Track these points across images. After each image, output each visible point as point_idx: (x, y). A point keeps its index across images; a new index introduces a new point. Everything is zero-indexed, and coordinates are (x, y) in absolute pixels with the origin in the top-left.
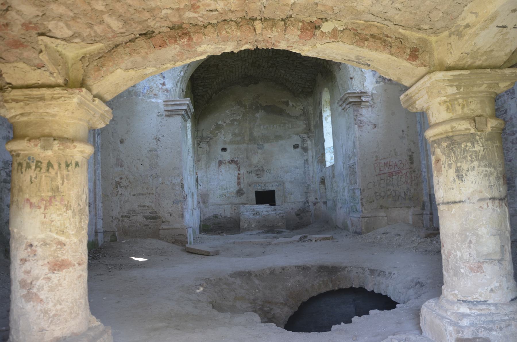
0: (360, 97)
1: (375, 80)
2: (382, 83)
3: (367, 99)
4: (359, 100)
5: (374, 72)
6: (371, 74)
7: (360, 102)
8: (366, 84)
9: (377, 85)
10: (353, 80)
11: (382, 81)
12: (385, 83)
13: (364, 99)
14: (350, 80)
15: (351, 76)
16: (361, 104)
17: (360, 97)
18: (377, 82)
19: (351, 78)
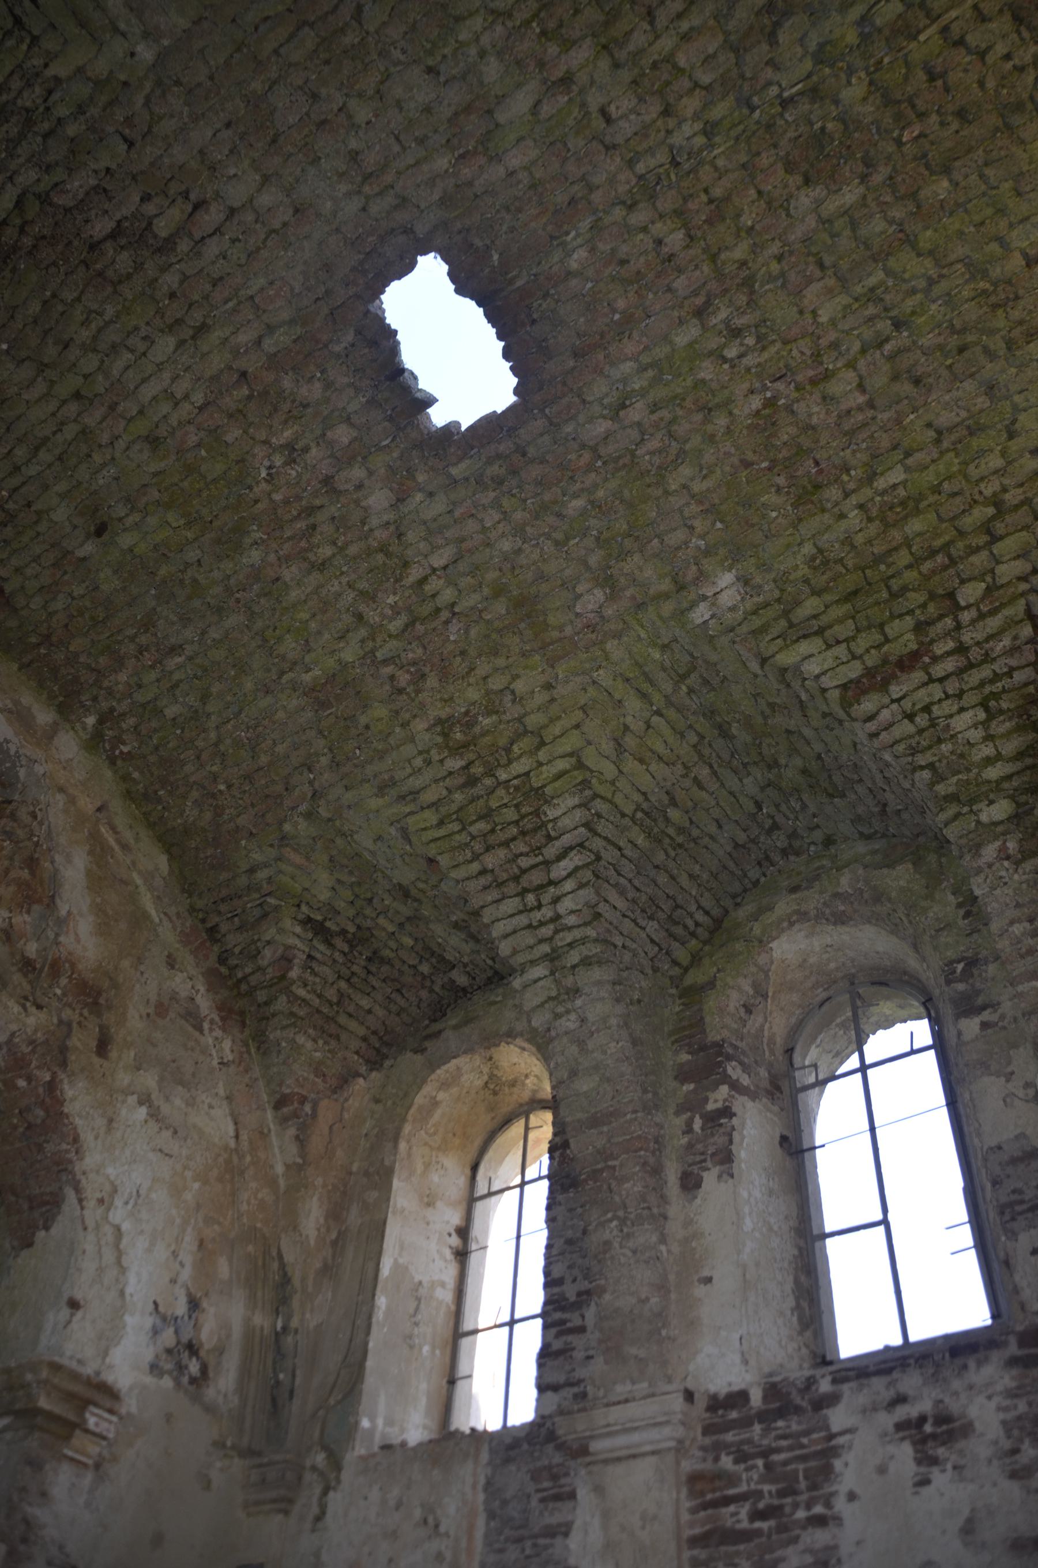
0: (86, 1403)
1: (149, 1355)
2: (167, 1382)
3: (103, 1428)
4: (71, 1416)
5: (158, 1322)
6: (149, 1322)
7: (69, 1427)
8: (118, 1356)
9: (149, 1380)
10: (80, 1314)
11: (170, 1373)
12: (178, 1384)
13: (92, 1421)
14: (65, 1312)
15: (78, 1296)
16: (68, 1438)
17: (84, 1404)
18: (154, 1368)
19: (74, 1305)
